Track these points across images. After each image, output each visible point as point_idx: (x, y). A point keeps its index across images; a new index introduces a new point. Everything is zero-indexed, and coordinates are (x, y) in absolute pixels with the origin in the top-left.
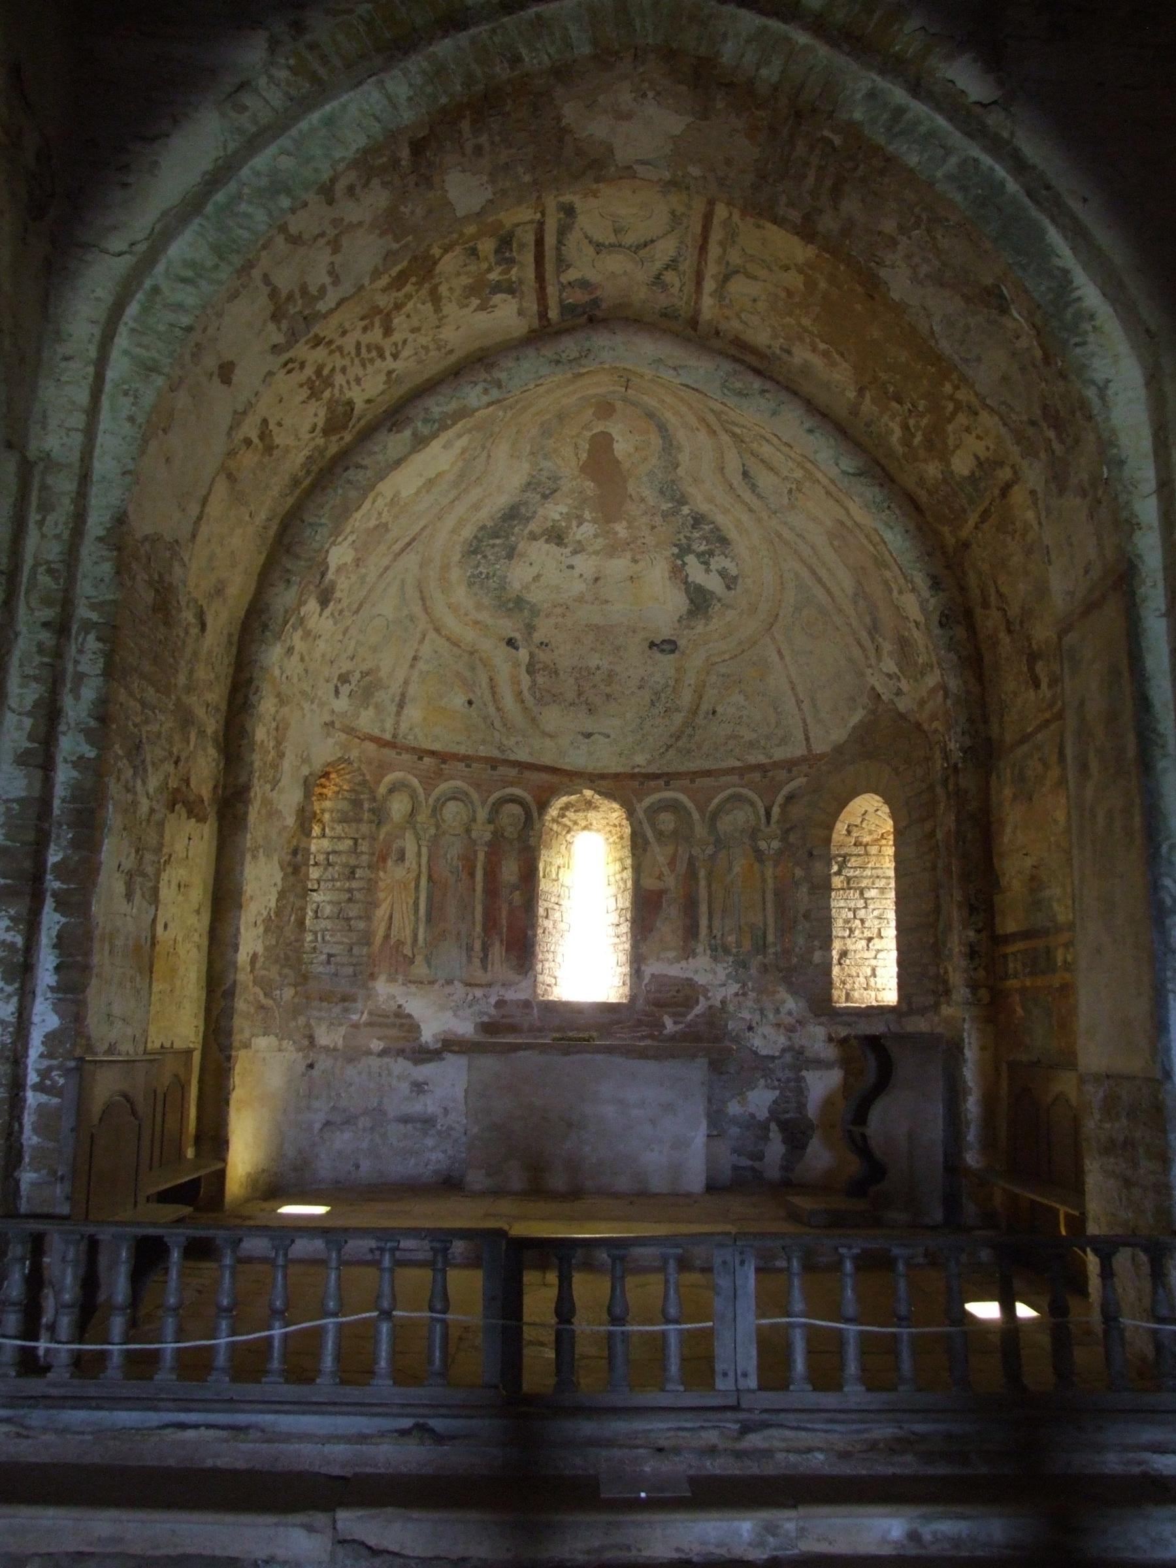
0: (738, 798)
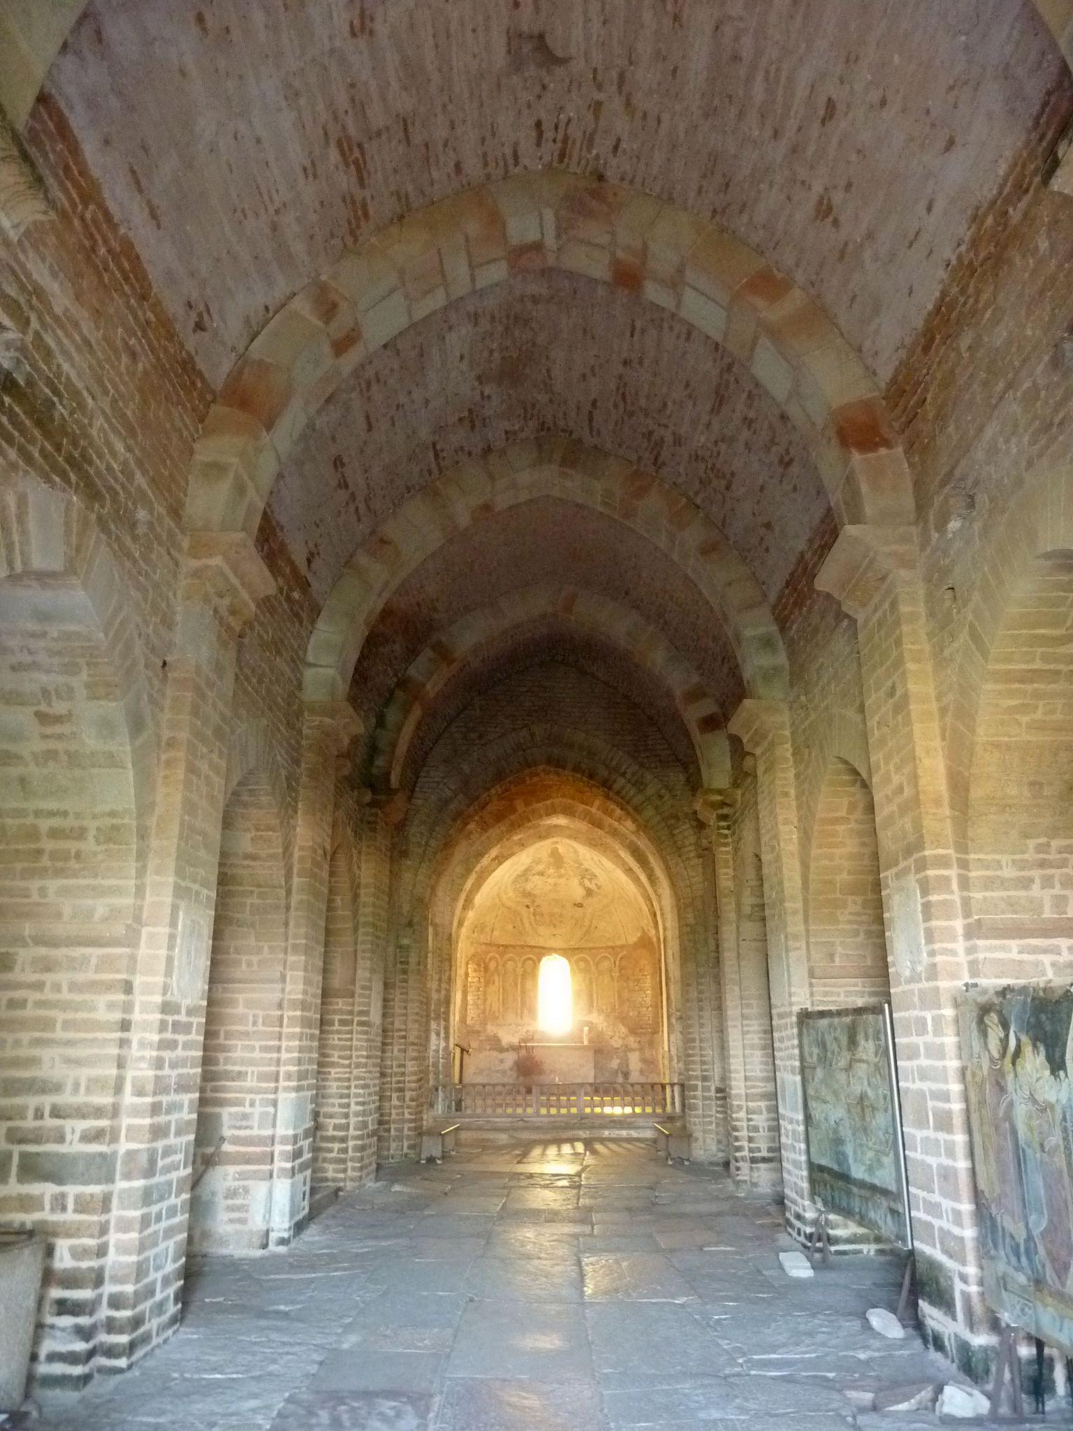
0: (605, 957)
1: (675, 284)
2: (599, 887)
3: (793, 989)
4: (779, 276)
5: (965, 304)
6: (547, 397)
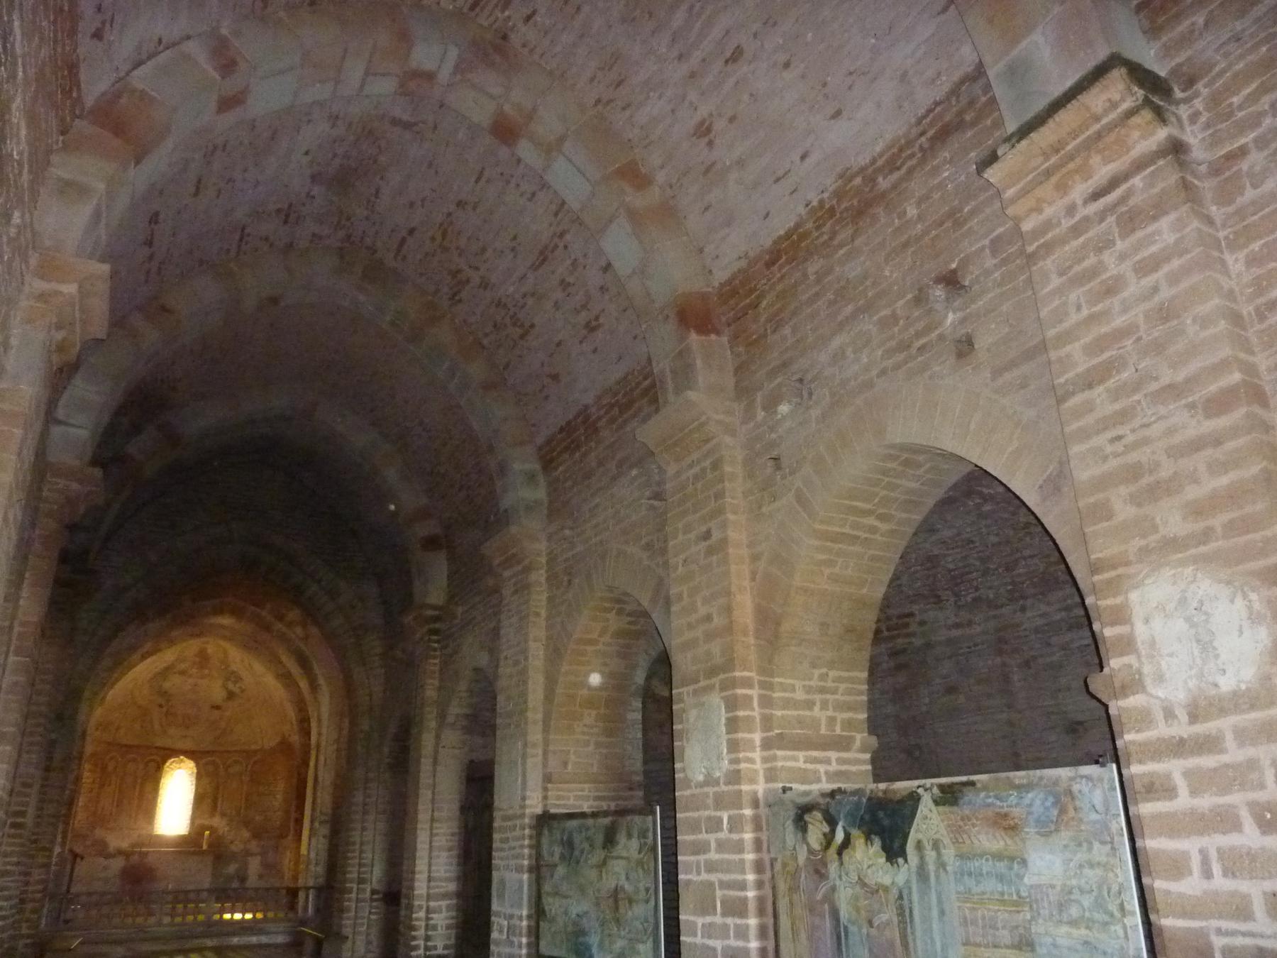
1: (551, 149)
2: (243, 691)
3: (528, 793)
4: (643, 171)
5: (817, 238)
6: (365, 213)
